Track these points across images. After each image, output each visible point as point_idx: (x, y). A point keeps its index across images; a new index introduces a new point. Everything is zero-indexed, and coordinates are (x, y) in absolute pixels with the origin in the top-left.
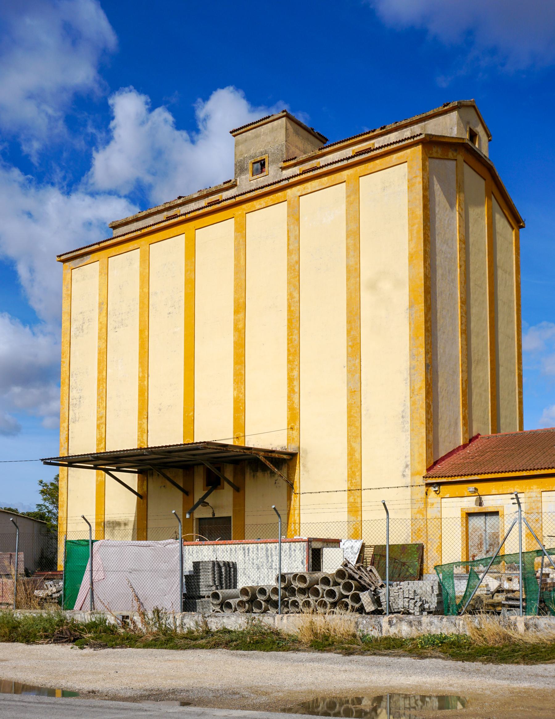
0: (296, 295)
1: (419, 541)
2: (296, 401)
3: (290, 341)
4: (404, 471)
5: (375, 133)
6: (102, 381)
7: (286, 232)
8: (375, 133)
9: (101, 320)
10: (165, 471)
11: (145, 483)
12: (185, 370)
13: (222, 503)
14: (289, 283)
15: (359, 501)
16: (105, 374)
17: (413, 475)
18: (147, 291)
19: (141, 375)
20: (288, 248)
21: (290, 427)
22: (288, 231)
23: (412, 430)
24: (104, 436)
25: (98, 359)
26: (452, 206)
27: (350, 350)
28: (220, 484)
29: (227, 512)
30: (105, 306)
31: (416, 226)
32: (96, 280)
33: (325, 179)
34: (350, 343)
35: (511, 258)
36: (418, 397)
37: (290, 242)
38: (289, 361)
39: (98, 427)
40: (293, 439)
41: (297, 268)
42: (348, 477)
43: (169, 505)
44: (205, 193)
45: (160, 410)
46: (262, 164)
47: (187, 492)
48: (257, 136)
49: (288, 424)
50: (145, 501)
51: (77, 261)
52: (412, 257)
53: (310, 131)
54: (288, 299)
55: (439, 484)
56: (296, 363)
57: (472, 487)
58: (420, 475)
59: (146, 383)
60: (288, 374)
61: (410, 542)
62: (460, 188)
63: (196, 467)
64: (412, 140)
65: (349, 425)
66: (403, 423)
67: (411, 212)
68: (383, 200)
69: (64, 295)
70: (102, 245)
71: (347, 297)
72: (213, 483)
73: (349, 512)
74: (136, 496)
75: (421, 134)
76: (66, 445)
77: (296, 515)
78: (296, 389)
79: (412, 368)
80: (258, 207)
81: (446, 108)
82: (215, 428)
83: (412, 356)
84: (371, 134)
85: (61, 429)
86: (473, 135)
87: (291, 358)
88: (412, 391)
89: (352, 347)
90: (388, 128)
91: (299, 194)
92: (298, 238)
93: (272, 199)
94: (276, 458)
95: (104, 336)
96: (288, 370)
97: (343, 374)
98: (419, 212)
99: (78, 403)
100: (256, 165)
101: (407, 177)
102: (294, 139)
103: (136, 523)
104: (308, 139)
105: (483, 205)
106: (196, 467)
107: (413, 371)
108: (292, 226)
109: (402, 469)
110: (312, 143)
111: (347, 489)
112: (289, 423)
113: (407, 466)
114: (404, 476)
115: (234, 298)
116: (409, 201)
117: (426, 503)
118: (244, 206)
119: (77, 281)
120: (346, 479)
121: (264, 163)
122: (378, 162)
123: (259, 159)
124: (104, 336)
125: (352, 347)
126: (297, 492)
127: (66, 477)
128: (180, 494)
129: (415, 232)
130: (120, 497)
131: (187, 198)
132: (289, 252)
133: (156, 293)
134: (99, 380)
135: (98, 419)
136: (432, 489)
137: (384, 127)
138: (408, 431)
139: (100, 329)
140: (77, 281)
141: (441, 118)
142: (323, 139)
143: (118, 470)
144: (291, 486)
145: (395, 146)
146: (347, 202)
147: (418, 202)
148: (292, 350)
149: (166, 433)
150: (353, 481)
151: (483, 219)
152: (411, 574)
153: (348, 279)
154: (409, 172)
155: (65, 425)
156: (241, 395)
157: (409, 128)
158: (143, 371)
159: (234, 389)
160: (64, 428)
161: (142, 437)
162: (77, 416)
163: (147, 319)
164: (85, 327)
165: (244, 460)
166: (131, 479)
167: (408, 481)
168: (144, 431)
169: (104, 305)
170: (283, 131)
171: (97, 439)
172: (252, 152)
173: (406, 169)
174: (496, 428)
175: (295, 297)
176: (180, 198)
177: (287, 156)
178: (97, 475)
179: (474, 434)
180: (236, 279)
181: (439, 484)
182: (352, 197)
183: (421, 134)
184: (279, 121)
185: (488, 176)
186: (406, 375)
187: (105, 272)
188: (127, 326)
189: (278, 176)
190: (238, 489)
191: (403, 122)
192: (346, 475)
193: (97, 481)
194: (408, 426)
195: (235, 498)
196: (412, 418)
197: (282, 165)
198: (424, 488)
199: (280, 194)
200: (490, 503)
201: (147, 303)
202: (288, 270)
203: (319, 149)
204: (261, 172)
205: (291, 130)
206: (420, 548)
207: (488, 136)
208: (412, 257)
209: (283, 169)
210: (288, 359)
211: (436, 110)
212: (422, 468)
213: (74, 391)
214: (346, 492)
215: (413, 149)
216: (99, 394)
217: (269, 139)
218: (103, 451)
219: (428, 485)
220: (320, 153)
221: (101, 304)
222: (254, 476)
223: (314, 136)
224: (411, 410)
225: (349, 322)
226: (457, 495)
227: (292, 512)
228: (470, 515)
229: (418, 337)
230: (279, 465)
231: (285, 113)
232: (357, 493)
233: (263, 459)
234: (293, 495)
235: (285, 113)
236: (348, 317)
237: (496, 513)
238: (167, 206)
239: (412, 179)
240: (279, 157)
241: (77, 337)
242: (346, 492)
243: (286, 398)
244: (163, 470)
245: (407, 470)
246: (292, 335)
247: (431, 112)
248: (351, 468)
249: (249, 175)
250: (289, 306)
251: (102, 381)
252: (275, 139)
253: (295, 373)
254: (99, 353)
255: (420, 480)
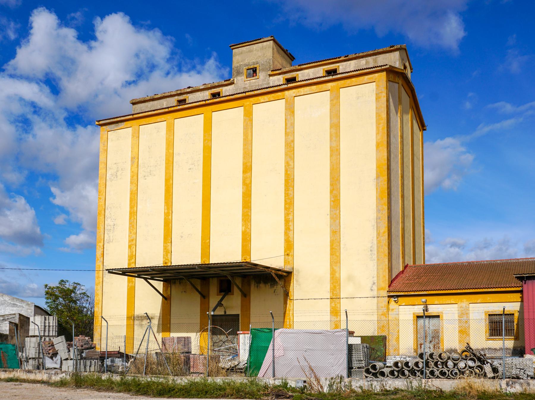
0: (291, 163)
1: (383, 334)
2: (291, 236)
3: (287, 195)
4: (372, 287)
5: (340, 59)
6: (133, 214)
7: (284, 120)
8: (340, 59)
9: (133, 170)
10: (193, 281)
11: (169, 288)
12: (203, 209)
13: (233, 305)
14: (286, 154)
15: (339, 307)
16: (135, 209)
17: (379, 289)
18: (172, 152)
19: (166, 211)
20: (286, 131)
21: (286, 253)
22: (286, 120)
23: (378, 260)
24: (134, 254)
25: (130, 198)
26: (397, 113)
27: (332, 203)
28: (230, 291)
29: (236, 311)
30: (137, 160)
31: (382, 125)
32: (129, 141)
33: (314, 87)
34: (333, 199)
35: (419, 149)
36: (382, 238)
37: (287, 127)
38: (286, 209)
39: (130, 247)
40: (289, 262)
41: (292, 145)
42: (331, 289)
43: (189, 306)
44: (209, 86)
45: (182, 237)
46: (255, 70)
47: (204, 296)
48: (250, 51)
49: (285, 252)
50: (169, 302)
51: (113, 126)
52: (378, 145)
53: (285, 52)
54: (285, 166)
55: (398, 296)
56: (291, 210)
57: (424, 299)
58: (384, 290)
59: (170, 217)
60: (285, 217)
61: (377, 335)
62: (400, 102)
63: (211, 279)
64: (380, 68)
65: (331, 254)
66: (371, 254)
67: (378, 115)
68: (361, 104)
69: (101, 150)
70: (135, 116)
71: (330, 168)
72: (226, 289)
73: (331, 312)
74: (161, 297)
75: (386, 65)
76: (102, 259)
77: (291, 315)
78: (291, 228)
79: (378, 218)
80: (262, 101)
81: (392, 49)
82: (226, 252)
83: (378, 211)
84: (338, 60)
85: (98, 247)
86: (405, 68)
87: (287, 206)
88: (378, 234)
89: (334, 201)
90: (350, 57)
91: (294, 95)
92: (293, 124)
93: (273, 97)
94: (280, 275)
95: (135, 180)
96: (285, 214)
97: (327, 220)
98: (384, 116)
99: (112, 229)
100: (249, 71)
101: (375, 92)
102: (277, 55)
103: (161, 317)
104: (284, 57)
105: (409, 113)
106: (211, 279)
107: (379, 221)
108: (288, 116)
109: (370, 285)
110: (286, 60)
111: (329, 297)
112: (285, 251)
113: (374, 283)
114: (372, 290)
115: (243, 162)
116: (376, 108)
117: (388, 309)
118: (251, 99)
119: (112, 140)
120: (329, 290)
121: (256, 70)
122: (354, 79)
123: (252, 67)
124: (135, 180)
125: (334, 201)
126: (292, 298)
127: (101, 283)
128: (198, 297)
129: (381, 128)
130: (149, 298)
131: (196, 89)
132: (286, 134)
133: (179, 154)
134: (130, 213)
135: (129, 241)
136: (392, 299)
137: (347, 56)
138: (374, 260)
139: (132, 177)
140: (112, 140)
141: (387, 55)
142: (292, 58)
143: (152, 279)
144: (287, 294)
145: (365, 71)
146: (330, 104)
147: (383, 109)
148: (288, 201)
149: (187, 255)
150: (335, 292)
151: (409, 123)
152: (379, 356)
153: (331, 156)
154: (377, 89)
155: (101, 244)
156: (248, 230)
157: (365, 59)
158: (168, 209)
159: (243, 225)
160: (100, 246)
161: (167, 256)
162: (111, 238)
163: (171, 172)
164: (118, 174)
165: (250, 275)
166: (159, 285)
167: (375, 293)
168: (168, 252)
169: (135, 160)
170: (271, 50)
171: (128, 256)
172: (246, 62)
173: (375, 87)
174: (414, 262)
175: (290, 165)
176: (189, 87)
177: (273, 67)
178: (129, 281)
179: (406, 264)
180: (244, 149)
181: (398, 296)
182: (335, 102)
183: (386, 65)
184: (268, 43)
185: (411, 96)
186: (374, 222)
187: (136, 136)
188: (155, 175)
189: (266, 80)
190: (245, 295)
191: (361, 54)
192: (329, 288)
193: (128, 286)
194: (375, 257)
195: (202, 304)
196: (378, 252)
197: (270, 73)
198: (387, 299)
199: (279, 94)
200: (433, 310)
201: (172, 160)
202: (285, 146)
203: (299, 66)
204: (253, 76)
205: (275, 50)
206: (384, 338)
207: (411, 69)
208: (378, 145)
209: (270, 75)
210: (285, 207)
211: (385, 49)
212: (385, 284)
213: (109, 220)
214: (329, 300)
215: (379, 74)
216: (130, 223)
217: (260, 54)
218: (169, 265)
219: (389, 297)
220: (299, 68)
221: (133, 159)
222: (257, 287)
223: (287, 55)
224: (377, 246)
225: (331, 185)
226: (410, 304)
227: (287, 312)
228: (418, 317)
229: (383, 199)
230: (275, 280)
231: (272, 38)
232: (338, 300)
233: (274, 275)
234: (288, 301)
235: (272, 38)
236: (331, 182)
237: (438, 317)
238: (179, 92)
239: (378, 94)
240: (267, 67)
241: (111, 180)
242: (329, 300)
243: (283, 234)
244: (190, 280)
245: (374, 286)
246: (288, 190)
247: (381, 50)
248: (333, 284)
249: (244, 77)
250: (286, 171)
251: (133, 214)
252: (264, 54)
253: (291, 217)
254: (131, 194)
255: (385, 294)
